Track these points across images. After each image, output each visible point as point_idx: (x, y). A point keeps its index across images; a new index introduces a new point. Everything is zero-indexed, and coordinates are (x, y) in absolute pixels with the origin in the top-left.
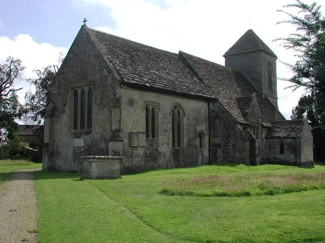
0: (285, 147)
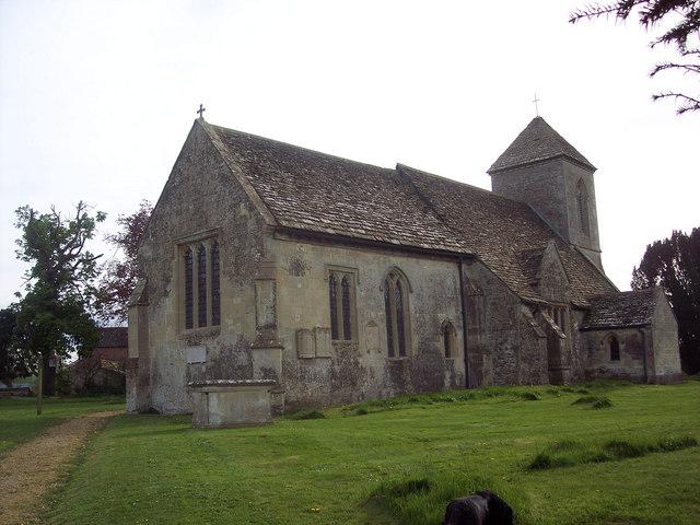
0: (622, 346)
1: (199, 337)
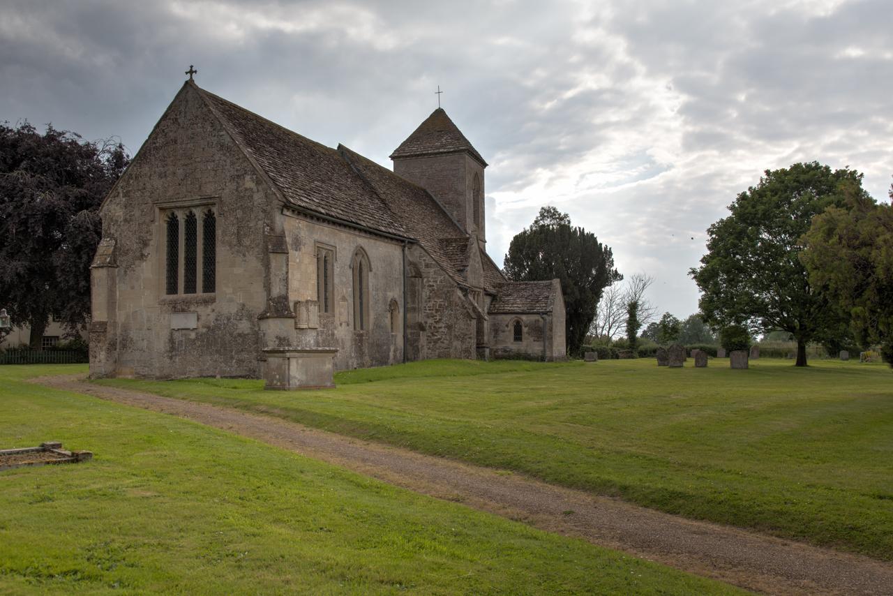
0: (525, 330)
1: (187, 303)
